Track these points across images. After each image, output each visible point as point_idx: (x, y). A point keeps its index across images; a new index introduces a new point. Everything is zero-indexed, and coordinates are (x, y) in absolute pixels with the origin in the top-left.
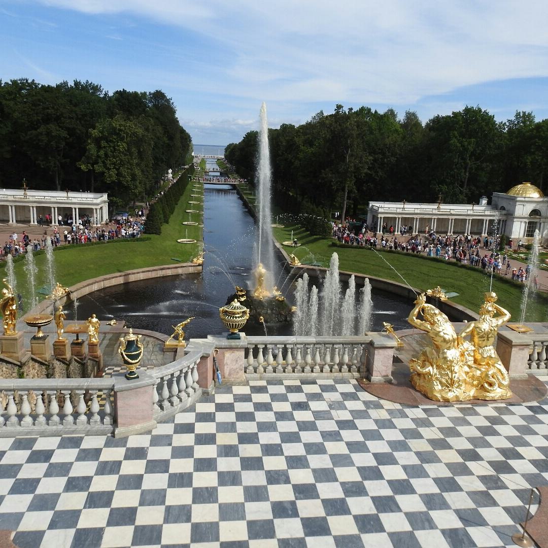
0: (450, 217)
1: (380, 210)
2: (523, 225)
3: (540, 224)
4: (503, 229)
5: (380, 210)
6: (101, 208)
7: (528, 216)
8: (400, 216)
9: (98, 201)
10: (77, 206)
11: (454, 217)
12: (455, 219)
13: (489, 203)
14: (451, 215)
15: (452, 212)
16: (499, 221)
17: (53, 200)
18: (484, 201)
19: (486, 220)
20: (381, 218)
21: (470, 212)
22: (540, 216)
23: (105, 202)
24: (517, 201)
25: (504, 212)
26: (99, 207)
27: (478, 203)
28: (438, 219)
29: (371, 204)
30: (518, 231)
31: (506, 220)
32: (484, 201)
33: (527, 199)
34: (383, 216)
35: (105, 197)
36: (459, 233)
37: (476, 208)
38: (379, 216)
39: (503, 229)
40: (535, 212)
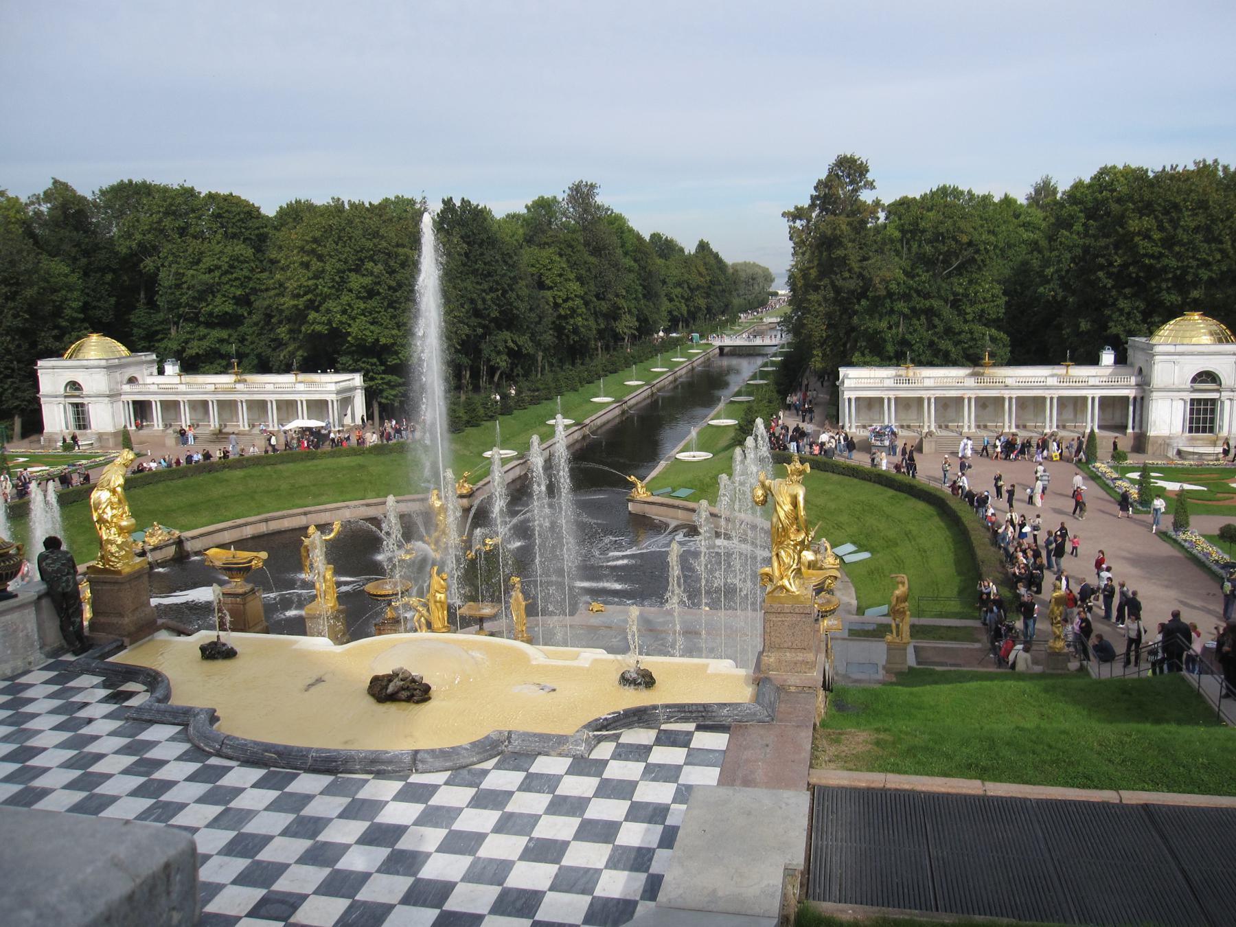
0: (1006, 394)
3: (1222, 403)
4: (1137, 418)
5: (847, 383)
6: (346, 402)
7: (1188, 385)
8: (892, 394)
9: (333, 387)
10: (304, 397)
11: (1016, 394)
12: (1018, 398)
13: (1121, 360)
15: (1009, 382)
16: (1135, 398)
17: (270, 387)
18: (1108, 357)
19: (1093, 399)
20: (850, 399)
21: (1052, 381)
23: (355, 388)
26: (333, 397)
27: (1094, 361)
28: (977, 399)
29: (843, 371)
30: (1167, 418)
31: (1142, 398)
32: (1108, 357)
33: (1180, 349)
34: (853, 395)
35: (357, 379)
38: (847, 395)
39: (1137, 418)
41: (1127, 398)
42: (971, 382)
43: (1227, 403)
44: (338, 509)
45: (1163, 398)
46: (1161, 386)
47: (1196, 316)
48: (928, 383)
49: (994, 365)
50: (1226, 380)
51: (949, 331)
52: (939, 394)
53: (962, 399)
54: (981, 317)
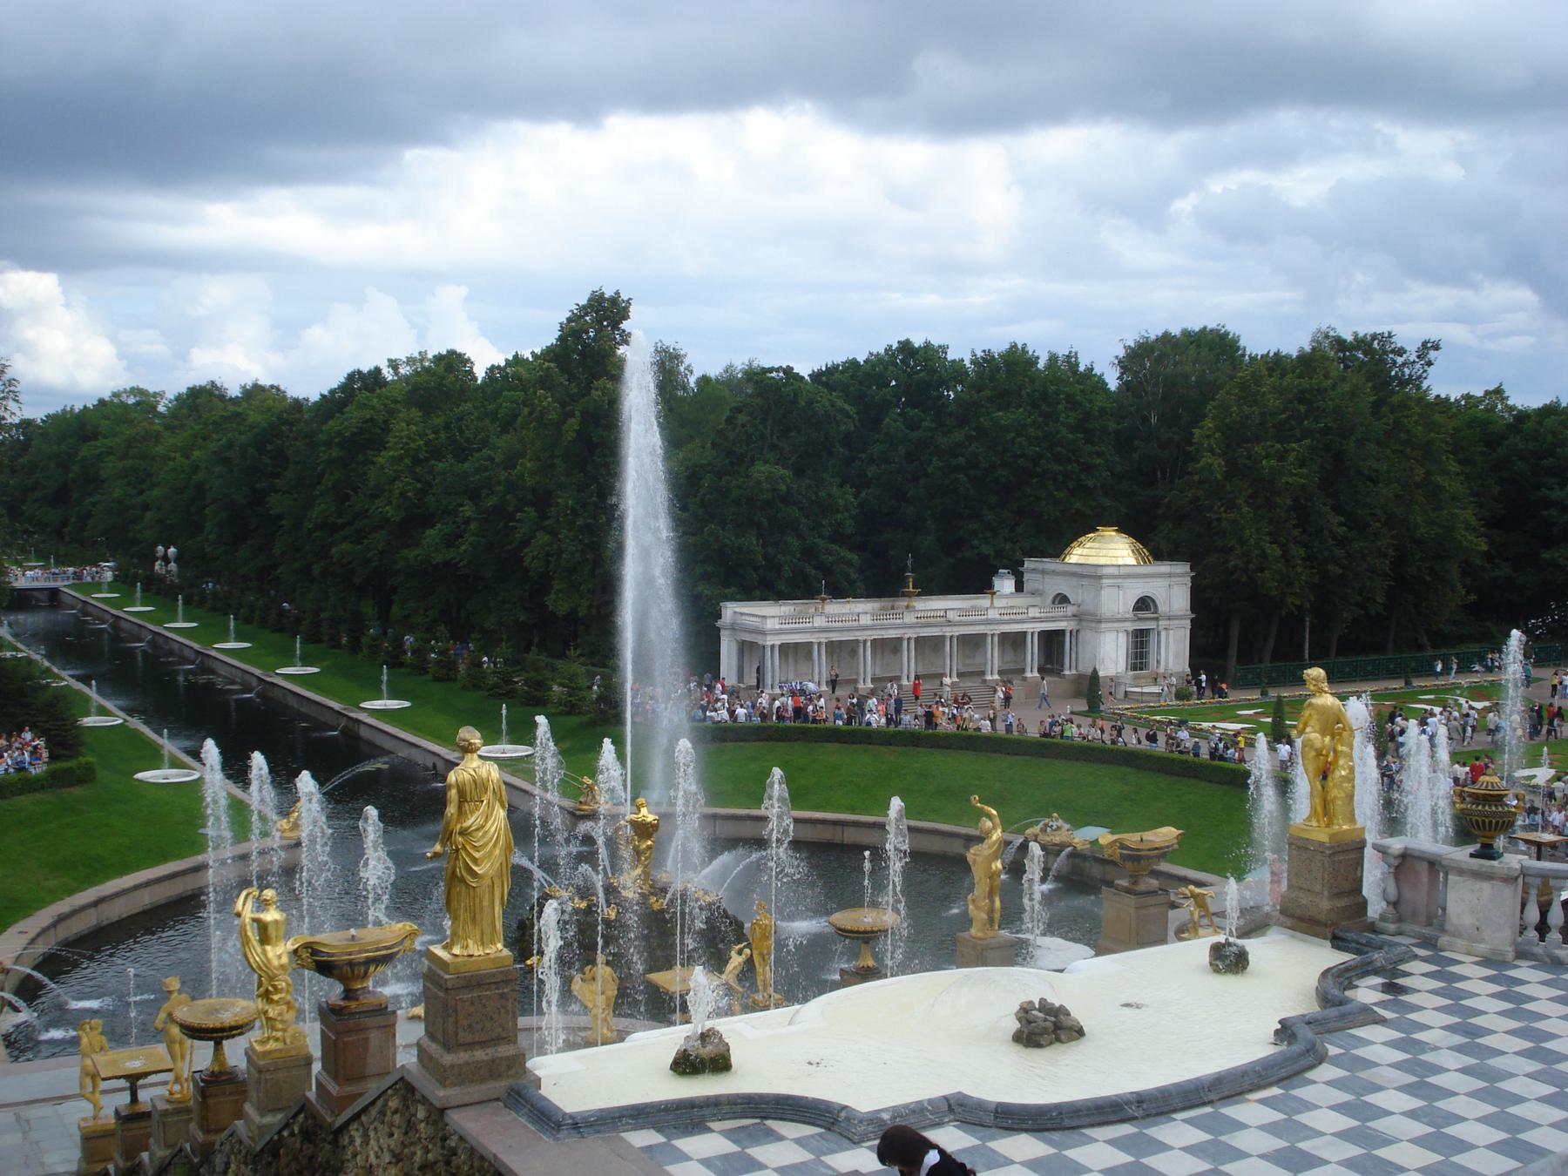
0: (948, 631)
1: (771, 624)
2: (1123, 638)
7: (1130, 615)
8: (823, 638)
13: (1019, 587)
14: (949, 623)
15: (951, 615)
18: (1005, 584)
20: (773, 647)
22: (1156, 612)
24: (1101, 577)
25: (1070, 610)
28: (917, 639)
36: (973, 674)
37: (997, 603)
40: (1144, 604)
41: (1061, 633)
42: (909, 618)
43: (1163, 634)
44: (136, 888)
45: (1110, 630)
46: (1108, 615)
47: (1110, 532)
48: (866, 620)
49: (919, 595)
50: (1163, 608)
51: (809, 553)
52: (877, 634)
53: (900, 640)
54: (837, 537)
